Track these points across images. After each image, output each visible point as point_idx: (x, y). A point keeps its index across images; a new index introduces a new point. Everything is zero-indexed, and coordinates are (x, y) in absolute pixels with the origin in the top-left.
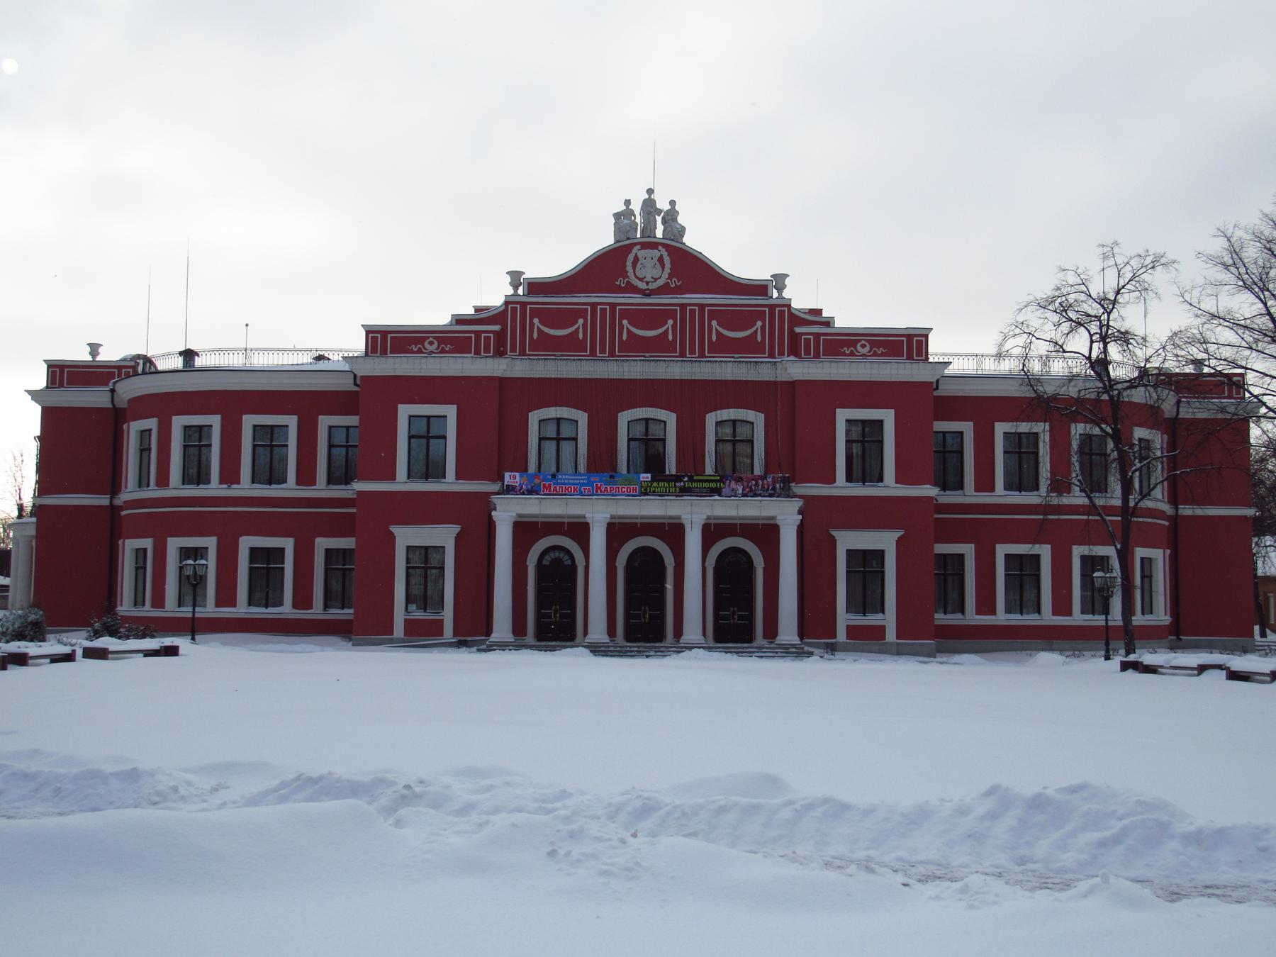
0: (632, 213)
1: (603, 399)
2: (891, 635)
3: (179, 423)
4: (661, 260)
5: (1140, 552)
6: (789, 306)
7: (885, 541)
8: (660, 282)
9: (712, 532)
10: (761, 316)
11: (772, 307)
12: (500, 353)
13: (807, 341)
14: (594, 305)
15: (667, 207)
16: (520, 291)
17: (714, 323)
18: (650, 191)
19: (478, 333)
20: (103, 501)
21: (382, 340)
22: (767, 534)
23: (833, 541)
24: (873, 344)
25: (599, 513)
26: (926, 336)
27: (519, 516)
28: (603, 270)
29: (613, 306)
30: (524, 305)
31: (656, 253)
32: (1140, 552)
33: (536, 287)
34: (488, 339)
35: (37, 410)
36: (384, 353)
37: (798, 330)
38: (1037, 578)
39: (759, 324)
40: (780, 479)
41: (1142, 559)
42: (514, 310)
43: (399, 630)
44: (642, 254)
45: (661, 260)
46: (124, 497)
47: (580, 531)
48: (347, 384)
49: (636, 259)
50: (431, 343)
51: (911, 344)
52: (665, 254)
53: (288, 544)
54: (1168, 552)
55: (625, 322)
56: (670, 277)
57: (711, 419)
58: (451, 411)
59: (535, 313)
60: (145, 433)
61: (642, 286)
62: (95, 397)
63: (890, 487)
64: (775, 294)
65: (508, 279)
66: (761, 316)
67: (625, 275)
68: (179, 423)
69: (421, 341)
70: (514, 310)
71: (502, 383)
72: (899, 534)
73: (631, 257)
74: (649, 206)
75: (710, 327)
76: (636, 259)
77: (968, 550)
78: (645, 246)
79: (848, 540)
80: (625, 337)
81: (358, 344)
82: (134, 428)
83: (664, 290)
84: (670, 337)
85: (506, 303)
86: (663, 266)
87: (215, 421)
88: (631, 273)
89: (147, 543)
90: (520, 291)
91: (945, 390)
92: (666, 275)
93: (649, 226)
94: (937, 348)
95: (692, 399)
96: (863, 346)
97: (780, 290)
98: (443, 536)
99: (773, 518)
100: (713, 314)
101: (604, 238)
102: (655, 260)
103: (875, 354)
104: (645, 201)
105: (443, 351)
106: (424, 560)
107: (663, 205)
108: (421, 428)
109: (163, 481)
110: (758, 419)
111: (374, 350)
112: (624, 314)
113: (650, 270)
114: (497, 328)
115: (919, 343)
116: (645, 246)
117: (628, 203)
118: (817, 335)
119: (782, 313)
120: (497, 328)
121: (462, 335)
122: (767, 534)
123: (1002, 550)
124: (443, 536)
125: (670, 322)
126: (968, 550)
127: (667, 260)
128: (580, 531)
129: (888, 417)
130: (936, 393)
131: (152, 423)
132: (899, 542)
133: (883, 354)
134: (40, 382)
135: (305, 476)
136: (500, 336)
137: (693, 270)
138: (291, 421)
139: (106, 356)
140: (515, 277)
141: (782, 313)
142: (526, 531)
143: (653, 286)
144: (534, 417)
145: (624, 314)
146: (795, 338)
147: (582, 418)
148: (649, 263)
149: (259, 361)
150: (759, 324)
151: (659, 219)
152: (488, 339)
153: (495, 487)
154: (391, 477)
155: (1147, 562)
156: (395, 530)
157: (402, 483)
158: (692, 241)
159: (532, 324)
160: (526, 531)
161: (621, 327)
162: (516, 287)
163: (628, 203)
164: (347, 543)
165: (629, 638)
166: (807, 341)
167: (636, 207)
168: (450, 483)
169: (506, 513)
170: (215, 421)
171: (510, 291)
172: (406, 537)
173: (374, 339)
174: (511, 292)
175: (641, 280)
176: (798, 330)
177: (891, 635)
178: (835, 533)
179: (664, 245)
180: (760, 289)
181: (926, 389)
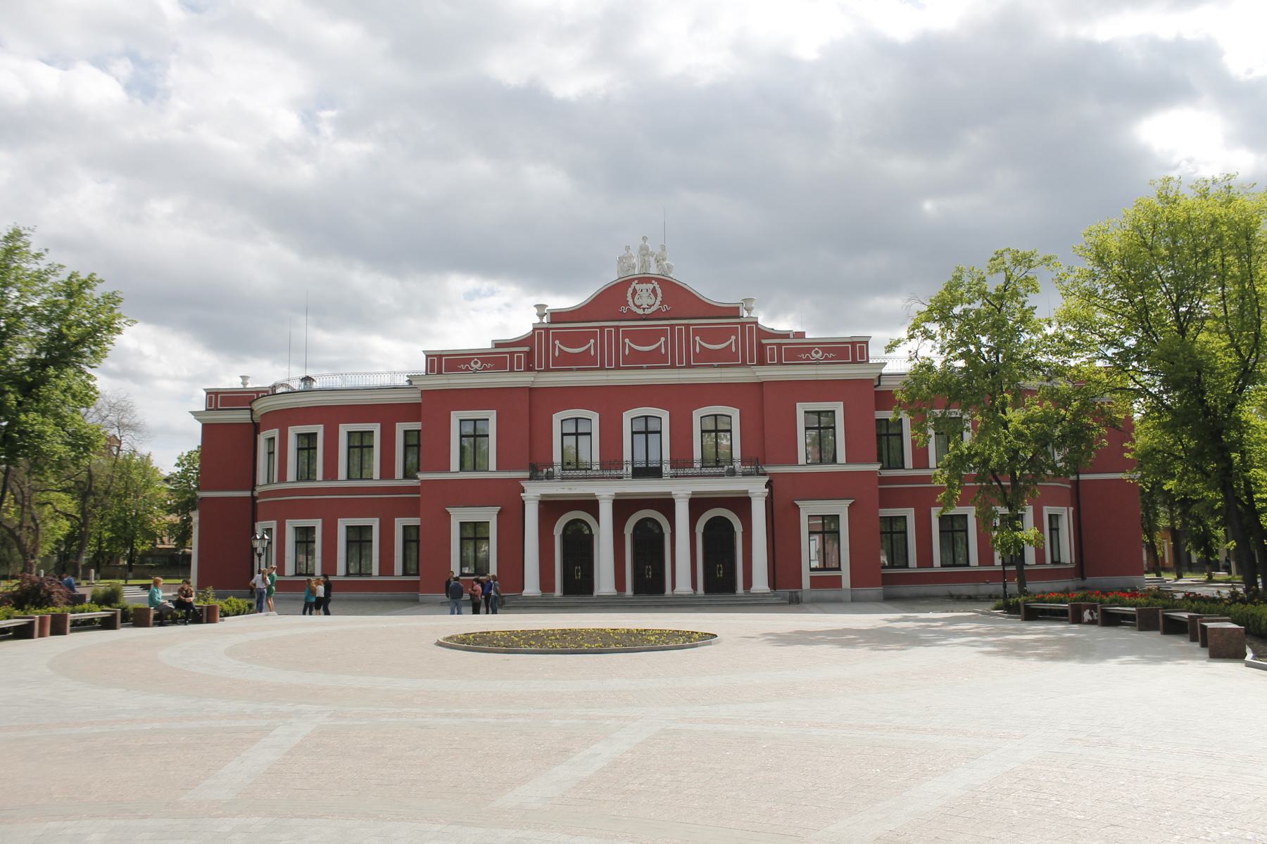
0: (632, 256)
1: (611, 402)
3: (293, 432)
4: (654, 290)
5: (1047, 510)
6: (756, 323)
7: (840, 508)
9: (698, 505)
10: (734, 331)
11: (743, 324)
12: (529, 369)
13: (772, 349)
14: (602, 328)
15: (658, 251)
16: (545, 320)
17: (697, 338)
18: (644, 239)
19: (512, 354)
20: (248, 494)
21: (440, 362)
22: (741, 504)
25: (605, 492)
26: (867, 343)
27: (543, 495)
28: (611, 301)
29: (617, 328)
30: (547, 330)
31: (650, 286)
33: (557, 316)
34: (519, 358)
35: (199, 425)
36: (440, 372)
37: (764, 341)
39: (733, 338)
40: (755, 461)
41: (1050, 516)
42: (540, 335)
44: (638, 287)
45: (654, 290)
46: (258, 489)
47: (591, 505)
48: (415, 397)
49: (635, 291)
50: (476, 363)
53: (375, 523)
54: (1071, 509)
55: (627, 340)
56: (662, 303)
57: (697, 415)
58: (492, 415)
59: (556, 336)
60: (271, 440)
61: (640, 312)
62: (242, 416)
63: (842, 464)
64: (746, 314)
65: (535, 310)
66: (734, 331)
68: (293, 432)
69: (468, 361)
70: (540, 335)
73: (630, 291)
74: (644, 252)
75: (695, 342)
76: (635, 291)
77: (910, 513)
78: (643, 280)
79: (809, 509)
81: (420, 366)
82: (262, 438)
83: (655, 316)
86: (656, 295)
87: (319, 430)
89: (273, 524)
90: (545, 320)
92: (658, 303)
93: (645, 264)
94: (875, 354)
95: (681, 400)
96: (817, 352)
97: (749, 310)
98: (489, 515)
99: (746, 492)
100: (696, 332)
101: (611, 276)
103: (826, 358)
104: (642, 248)
105: (485, 368)
106: (474, 534)
107: (653, 247)
108: (469, 429)
109: (283, 478)
110: (735, 413)
111: (432, 370)
112: (626, 334)
113: (645, 300)
114: (526, 349)
115: (862, 348)
116: (643, 280)
117: (628, 248)
118: (779, 345)
120: (526, 349)
121: (501, 356)
122: (741, 504)
124: (489, 515)
125: (663, 339)
126: (910, 513)
127: (659, 291)
128: (591, 505)
129: (839, 408)
130: (878, 389)
131: (275, 433)
132: (851, 507)
134: (201, 407)
135: (387, 472)
136: (529, 355)
137: (678, 298)
138: (376, 428)
140: (540, 307)
142: (551, 509)
143: (647, 312)
144: (557, 418)
145: (626, 334)
146: (761, 348)
147: (595, 417)
148: (644, 294)
150: (733, 338)
151: (652, 259)
152: (519, 358)
153: (527, 475)
154: (447, 469)
155: (1054, 518)
156: (449, 509)
157: (455, 471)
158: (679, 275)
160: (551, 509)
161: (624, 344)
162: (541, 316)
163: (628, 248)
164: (414, 521)
165: (637, 590)
166: (772, 349)
167: (635, 252)
168: (492, 472)
169: (533, 493)
170: (319, 430)
171: (537, 320)
172: (459, 516)
174: (537, 320)
175: (639, 307)
176: (764, 341)
179: (656, 279)
180: (733, 312)
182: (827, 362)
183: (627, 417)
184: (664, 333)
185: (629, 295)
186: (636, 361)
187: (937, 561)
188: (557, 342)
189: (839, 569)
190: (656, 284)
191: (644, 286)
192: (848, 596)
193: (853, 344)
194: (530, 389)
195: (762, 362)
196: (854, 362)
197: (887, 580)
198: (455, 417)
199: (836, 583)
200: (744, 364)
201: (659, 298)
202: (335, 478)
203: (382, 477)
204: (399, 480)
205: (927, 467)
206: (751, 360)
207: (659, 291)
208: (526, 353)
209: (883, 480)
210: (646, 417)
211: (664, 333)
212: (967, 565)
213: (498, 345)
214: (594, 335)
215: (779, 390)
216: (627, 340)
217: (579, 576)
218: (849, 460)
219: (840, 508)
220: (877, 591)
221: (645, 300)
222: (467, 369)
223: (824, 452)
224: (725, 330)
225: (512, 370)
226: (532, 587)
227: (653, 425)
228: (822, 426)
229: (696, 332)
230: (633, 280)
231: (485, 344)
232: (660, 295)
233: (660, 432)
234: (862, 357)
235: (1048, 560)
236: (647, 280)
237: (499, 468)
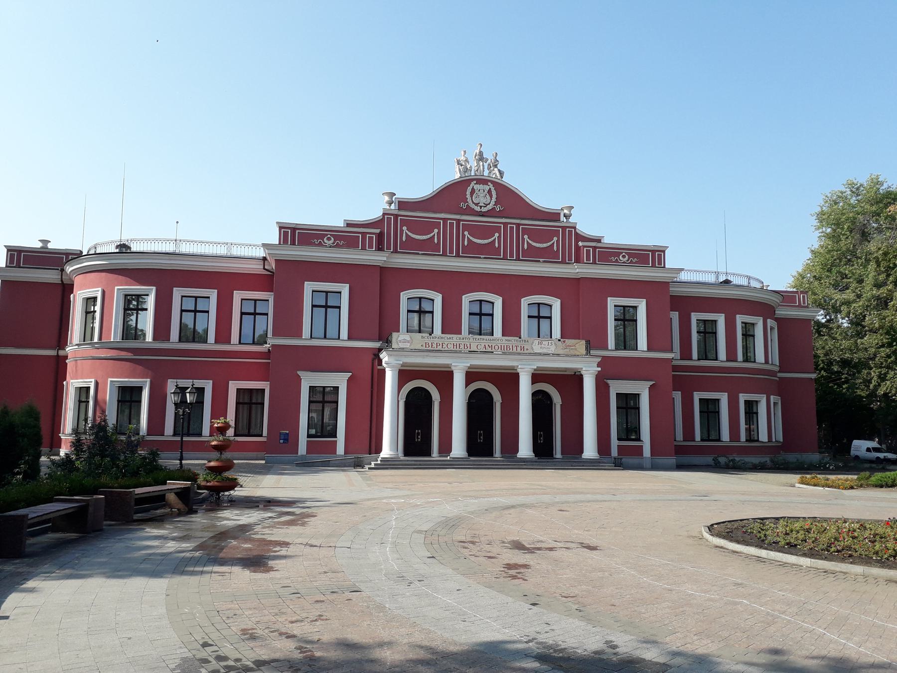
1: (453, 285)
2: (647, 452)
4: (490, 191)
5: (772, 398)
6: (575, 228)
8: (489, 207)
10: (556, 233)
11: (564, 228)
12: (380, 248)
13: (588, 252)
14: (445, 220)
16: (393, 207)
19: (364, 234)
21: (292, 234)
23: (607, 386)
24: (630, 255)
26: (664, 252)
28: (452, 195)
30: (396, 216)
31: (487, 188)
32: (772, 398)
33: (403, 205)
36: (293, 243)
38: (718, 413)
42: (389, 220)
43: (302, 449)
44: (477, 187)
45: (490, 191)
49: (473, 191)
50: (329, 239)
51: (652, 256)
52: (493, 189)
55: (466, 233)
58: (345, 289)
61: (477, 209)
67: (466, 201)
69: (322, 237)
71: (383, 271)
72: (652, 383)
75: (523, 239)
76: (473, 191)
79: (617, 387)
80: (466, 243)
81: (274, 238)
83: (490, 213)
84: (497, 245)
85: (384, 214)
86: (491, 197)
88: (469, 200)
91: (674, 290)
92: (493, 203)
95: (512, 288)
96: (624, 257)
97: (567, 217)
98: (340, 380)
102: (486, 192)
105: (338, 246)
106: (323, 398)
110: (556, 304)
111: (285, 242)
112: (466, 227)
113: (482, 199)
115: (660, 256)
118: (595, 248)
119: (570, 232)
120: (378, 231)
123: (697, 396)
124: (340, 380)
127: (494, 193)
129: (642, 306)
132: (651, 388)
133: (636, 263)
135: (223, 335)
136: (380, 236)
137: (510, 201)
138: (213, 294)
139: (50, 246)
141: (570, 232)
143: (484, 210)
144: (404, 296)
145: (466, 227)
146: (578, 248)
149: (185, 249)
151: (486, 165)
154: (299, 335)
157: (305, 339)
158: (509, 180)
159: (402, 231)
161: (464, 236)
166: (588, 252)
168: (344, 341)
172: (309, 380)
173: (286, 234)
175: (477, 204)
177: (647, 452)
178: (609, 382)
179: (492, 182)
180: (554, 216)
181: (664, 285)
182: (630, 264)
183: (466, 299)
184: (498, 229)
185: (468, 193)
186: (474, 251)
187: (698, 437)
188: (405, 228)
189: (638, 439)
190: (491, 186)
191: (481, 187)
192: (648, 464)
193: (653, 252)
194: (381, 268)
195: (578, 260)
196: (653, 266)
197: (680, 450)
198: (309, 287)
199: (639, 451)
200: (563, 262)
201: (494, 199)
202: (168, 339)
203: (217, 341)
204: (234, 345)
205: (690, 359)
206: (570, 259)
207: (494, 193)
208: (379, 233)
209: (676, 368)
210: (481, 301)
211: (498, 229)
212: (719, 440)
213: (349, 225)
214: (437, 225)
215: (601, 286)
216: (466, 233)
217: (419, 439)
218: (650, 348)
219: (642, 389)
220: (672, 460)
221: (482, 199)
222: (320, 244)
223: (626, 340)
224: (548, 231)
225: (363, 248)
226: (387, 451)
227: (486, 309)
228: (627, 318)
229: (525, 231)
230: (473, 180)
231: (337, 221)
232: (494, 196)
233: (492, 315)
234: (660, 263)
235: (743, 437)
236: (484, 182)
237: (350, 338)
